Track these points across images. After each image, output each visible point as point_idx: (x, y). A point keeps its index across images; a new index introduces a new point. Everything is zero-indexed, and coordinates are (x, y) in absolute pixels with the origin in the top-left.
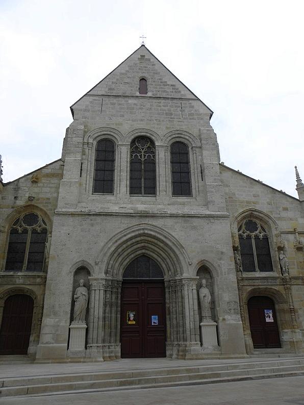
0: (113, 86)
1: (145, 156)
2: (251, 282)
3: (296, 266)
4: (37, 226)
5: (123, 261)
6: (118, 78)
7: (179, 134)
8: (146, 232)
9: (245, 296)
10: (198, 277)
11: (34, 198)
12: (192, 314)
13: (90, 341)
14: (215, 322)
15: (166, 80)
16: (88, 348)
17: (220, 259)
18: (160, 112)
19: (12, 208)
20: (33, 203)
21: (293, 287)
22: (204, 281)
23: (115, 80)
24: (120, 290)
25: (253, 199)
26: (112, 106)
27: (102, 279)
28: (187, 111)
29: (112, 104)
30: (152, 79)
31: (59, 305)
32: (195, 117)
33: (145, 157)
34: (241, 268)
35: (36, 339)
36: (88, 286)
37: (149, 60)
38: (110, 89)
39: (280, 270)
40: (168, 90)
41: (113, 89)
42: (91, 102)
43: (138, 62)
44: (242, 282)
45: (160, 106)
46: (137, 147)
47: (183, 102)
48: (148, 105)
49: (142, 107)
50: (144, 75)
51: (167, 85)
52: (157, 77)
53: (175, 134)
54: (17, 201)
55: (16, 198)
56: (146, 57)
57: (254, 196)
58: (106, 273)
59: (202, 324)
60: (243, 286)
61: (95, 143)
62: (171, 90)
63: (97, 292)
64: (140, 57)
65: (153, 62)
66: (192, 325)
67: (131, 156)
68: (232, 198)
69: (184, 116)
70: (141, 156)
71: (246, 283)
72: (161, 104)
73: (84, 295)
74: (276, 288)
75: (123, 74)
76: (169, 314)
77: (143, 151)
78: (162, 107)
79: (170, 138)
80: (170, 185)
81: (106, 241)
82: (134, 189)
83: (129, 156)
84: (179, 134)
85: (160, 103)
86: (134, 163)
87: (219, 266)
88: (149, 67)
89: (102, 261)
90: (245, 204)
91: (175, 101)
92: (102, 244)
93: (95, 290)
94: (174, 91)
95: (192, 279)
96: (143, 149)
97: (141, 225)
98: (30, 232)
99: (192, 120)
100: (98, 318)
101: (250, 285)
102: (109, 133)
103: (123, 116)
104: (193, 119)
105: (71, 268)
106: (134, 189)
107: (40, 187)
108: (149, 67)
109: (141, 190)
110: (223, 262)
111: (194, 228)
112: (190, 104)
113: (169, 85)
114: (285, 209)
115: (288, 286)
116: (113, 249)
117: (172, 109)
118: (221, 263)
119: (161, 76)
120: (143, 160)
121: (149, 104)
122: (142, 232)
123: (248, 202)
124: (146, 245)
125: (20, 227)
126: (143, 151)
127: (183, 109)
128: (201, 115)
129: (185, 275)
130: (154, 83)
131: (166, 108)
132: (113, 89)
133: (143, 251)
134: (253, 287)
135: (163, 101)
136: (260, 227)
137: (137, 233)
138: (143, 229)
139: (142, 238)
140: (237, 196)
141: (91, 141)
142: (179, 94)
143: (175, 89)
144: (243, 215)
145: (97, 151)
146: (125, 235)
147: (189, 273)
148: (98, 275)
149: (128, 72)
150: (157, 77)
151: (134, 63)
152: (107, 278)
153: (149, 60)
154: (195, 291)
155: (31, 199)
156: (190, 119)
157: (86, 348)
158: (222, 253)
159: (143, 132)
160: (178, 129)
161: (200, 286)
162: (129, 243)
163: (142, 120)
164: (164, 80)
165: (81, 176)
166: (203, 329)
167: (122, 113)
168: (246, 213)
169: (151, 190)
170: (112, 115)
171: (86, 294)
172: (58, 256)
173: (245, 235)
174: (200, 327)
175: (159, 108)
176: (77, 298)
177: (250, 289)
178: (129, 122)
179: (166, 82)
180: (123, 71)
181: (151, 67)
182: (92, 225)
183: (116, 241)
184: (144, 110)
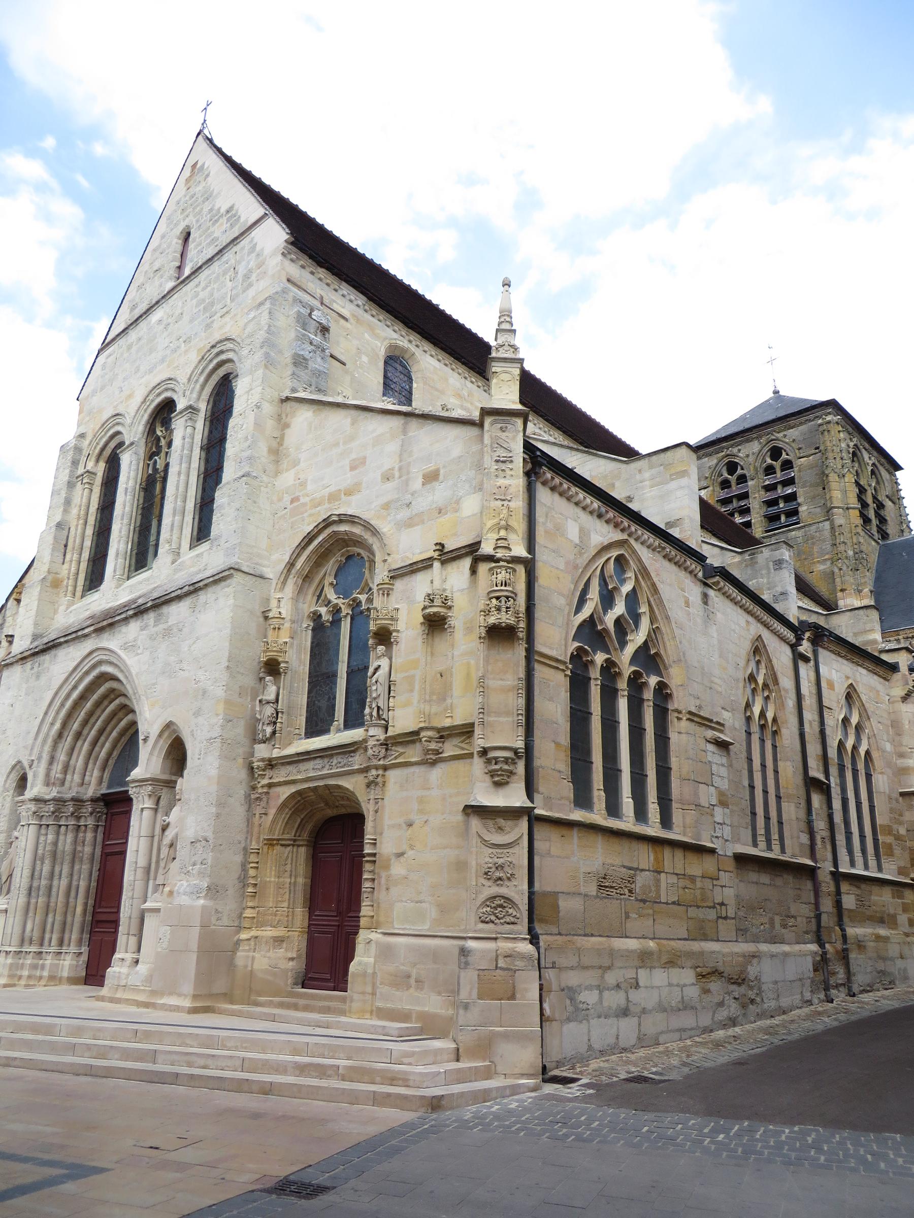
3: (416, 696)
5: (97, 749)
7: (218, 354)
9: (269, 817)
17: (197, 714)
21: (393, 776)
27: (30, 800)
44: (268, 773)
53: (211, 361)
58: (47, 784)
60: (270, 786)
71: (280, 775)
74: (347, 783)
79: (202, 379)
84: (218, 354)
89: (40, 758)
90: (327, 505)
97: (95, 655)
105: (6, 781)
110: (201, 720)
114: (431, 477)
115: (374, 772)
116: (58, 725)
121: (180, 304)
134: (293, 789)
140: (310, 487)
144: (311, 547)
146: (75, 687)
148: (35, 789)
162: (89, 705)
168: (320, 538)
177: (285, 792)
183: (62, 705)
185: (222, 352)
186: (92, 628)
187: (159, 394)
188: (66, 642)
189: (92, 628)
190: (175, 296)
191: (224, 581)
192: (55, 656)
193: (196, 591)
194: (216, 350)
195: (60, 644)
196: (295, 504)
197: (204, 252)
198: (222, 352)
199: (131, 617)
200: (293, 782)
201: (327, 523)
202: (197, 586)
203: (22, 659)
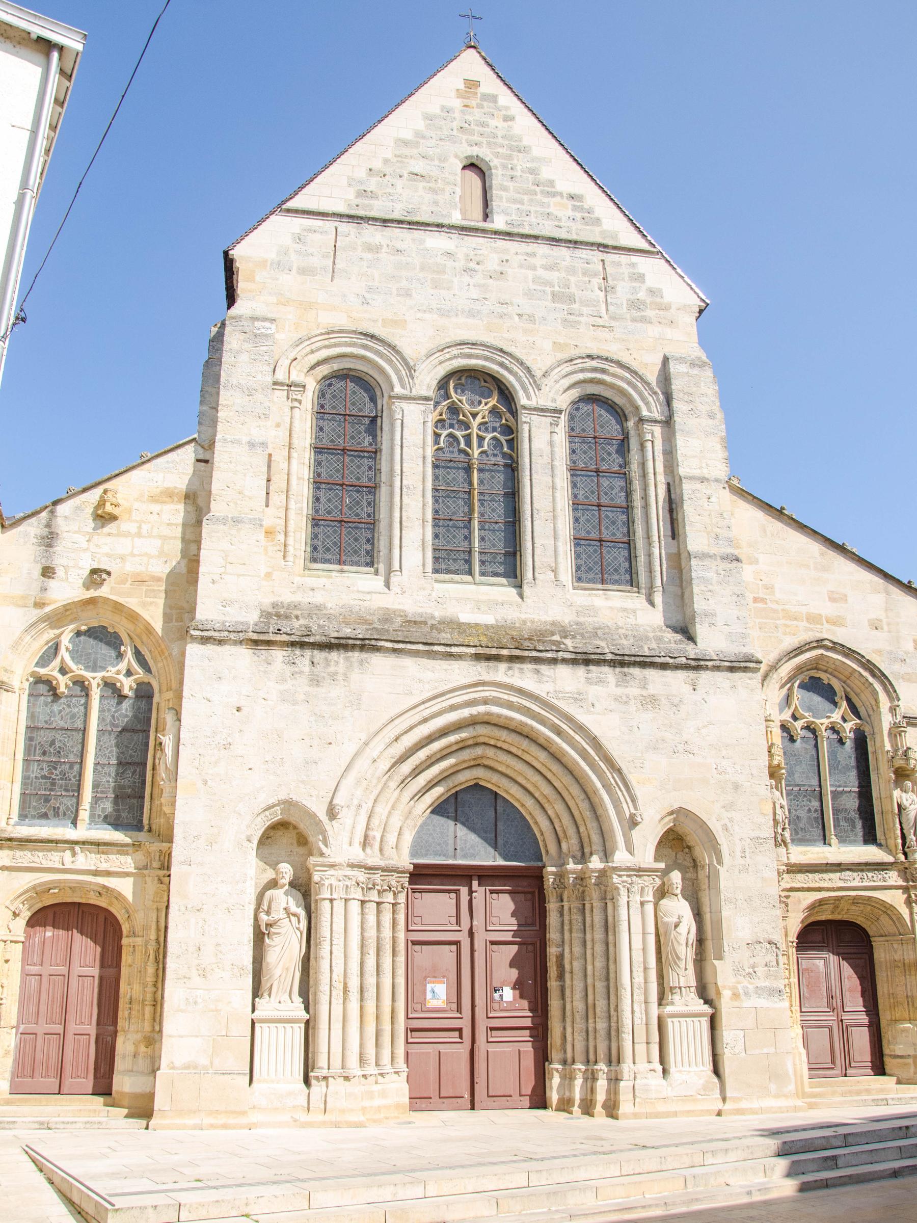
0: (373, 184)
1: (481, 439)
2: (813, 880)
4: (118, 673)
6: (389, 155)
7: (595, 370)
8: (495, 709)
10: (662, 865)
11: (109, 573)
12: (639, 978)
13: (322, 1061)
14: (706, 1002)
15: (551, 177)
16: (313, 1082)
18: (533, 287)
19: (39, 605)
20: (104, 591)
22: (676, 877)
23: (377, 165)
24: (402, 898)
25: (827, 609)
26: (368, 256)
27: (352, 866)
28: (623, 291)
29: (374, 249)
30: (504, 167)
31: (218, 945)
32: (650, 313)
33: (480, 445)
34: (787, 834)
35: (142, 1049)
36: (303, 888)
37: (493, 99)
38: (363, 193)
39: (900, 841)
40: (560, 214)
41: (373, 196)
42: (299, 239)
43: (457, 103)
45: (534, 268)
46: (454, 410)
47: (611, 258)
48: (492, 264)
49: (472, 265)
50: (475, 151)
51: (554, 194)
52: (521, 163)
54: (52, 583)
55: (48, 572)
56: (483, 89)
57: (832, 599)
59: (669, 1009)
61: (312, 385)
62: (570, 213)
63: (339, 906)
64: (462, 86)
65: (507, 108)
66: (637, 1014)
67: (437, 436)
68: (763, 601)
69: (611, 308)
70: (468, 438)
71: (801, 880)
72: (538, 262)
73: (294, 915)
75: (406, 143)
76: (561, 976)
77: (475, 424)
78: (540, 272)
80: (566, 548)
81: (364, 737)
82: (450, 558)
83: (430, 439)
84: (595, 370)
85: (534, 255)
86: (450, 465)
87: (726, 829)
88: (493, 123)
90: (805, 624)
91: (583, 253)
92: (351, 748)
93: (331, 900)
94: (578, 215)
95: (640, 871)
96: (474, 415)
98: (96, 694)
99: (639, 325)
100: (346, 990)
101: (809, 889)
102: (362, 352)
103: (408, 294)
104: (644, 320)
106: (450, 558)
107: (127, 534)
108: (493, 123)
109: (468, 562)
111: (651, 702)
112: (633, 265)
113: (561, 194)
117: (573, 279)
118: (731, 820)
119: (533, 160)
120: (476, 453)
122: (482, 709)
123: (813, 619)
124: (490, 752)
125: (63, 671)
126: (475, 424)
127: (611, 282)
128: (667, 308)
129: (621, 857)
130: (511, 185)
131: (554, 276)
132: (373, 196)
133: (479, 773)
135: (542, 249)
136: (845, 703)
137: (466, 713)
138: (485, 702)
139: (481, 730)
141: (296, 377)
142: (597, 229)
143: (582, 209)
145: (321, 413)
146: (425, 720)
147: (639, 849)
148: (341, 845)
149: (423, 137)
150: (521, 163)
151: (443, 108)
152: (371, 862)
153: (493, 99)
154: (650, 908)
155: (97, 576)
156: (634, 320)
157: (307, 1081)
158: (736, 787)
159: (477, 357)
160: (594, 352)
161: (662, 893)
163: (471, 314)
164: (546, 173)
165: (267, 506)
166: (672, 1026)
167: (404, 283)
169: (510, 564)
170: (370, 289)
171: (302, 913)
172: (205, 782)
173: (799, 724)
174: (660, 1019)
175: (530, 274)
176: (269, 925)
178: (427, 316)
179: (551, 183)
180: (408, 135)
181: (501, 124)
182: (315, 681)
184: (479, 278)
185: (603, 371)
186: (472, 650)
187: (470, 356)
188: (395, 650)
189: (472, 650)
190: (481, 240)
191: (744, 672)
192: (361, 662)
193: (697, 668)
194: (594, 364)
195: (378, 649)
196: (760, 605)
197: (533, 219)
198: (603, 371)
199: (564, 661)
200: (819, 889)
201: (819, 643)
202: (702, 663)
203: (256, 642)
